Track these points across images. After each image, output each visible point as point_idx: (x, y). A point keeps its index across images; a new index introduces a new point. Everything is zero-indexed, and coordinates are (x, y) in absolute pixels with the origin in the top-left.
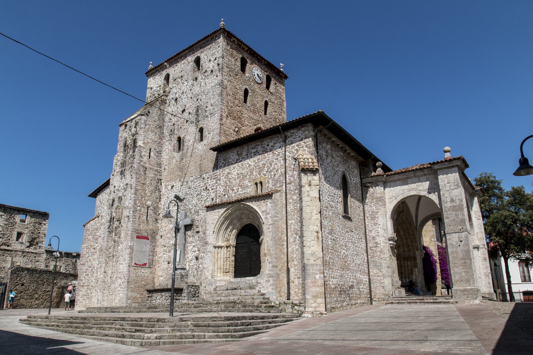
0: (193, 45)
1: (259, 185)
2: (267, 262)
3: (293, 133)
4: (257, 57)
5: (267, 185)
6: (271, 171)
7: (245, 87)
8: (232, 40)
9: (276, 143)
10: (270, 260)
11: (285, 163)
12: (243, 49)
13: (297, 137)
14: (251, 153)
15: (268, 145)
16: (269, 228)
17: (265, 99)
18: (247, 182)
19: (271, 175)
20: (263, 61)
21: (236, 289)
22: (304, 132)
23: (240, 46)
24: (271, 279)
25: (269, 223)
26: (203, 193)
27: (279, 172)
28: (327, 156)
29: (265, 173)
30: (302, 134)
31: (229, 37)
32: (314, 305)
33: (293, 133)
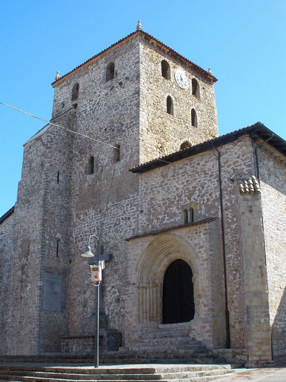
0: (105, 50)
1: (189, 213)
3: (228, 149)
4: (180, 60)
5: (199, 212)
6: (203, 196)
7: (167, 95)
8: (150, 42)
9: (208, 162)
11: (220, 184)
12: (164, 51)
13: (233, 153)
14: (179, 174)
15: (198, 164)
16: (203, 264)
17: (192, 108)
18: (174, 208)
19: (204, 200)
20: (187, 63)
21: (166, 337)
22: (241, 147)
23: (160, 48)
24: (207, 325)
25: (203, 258)
26: (121, 224)
27: (214, 196)
28: (269, 175)
29: (196, 197)
30: (239, 150)
31: (147, 39)
32: (259, 353)
33: (228, 149)
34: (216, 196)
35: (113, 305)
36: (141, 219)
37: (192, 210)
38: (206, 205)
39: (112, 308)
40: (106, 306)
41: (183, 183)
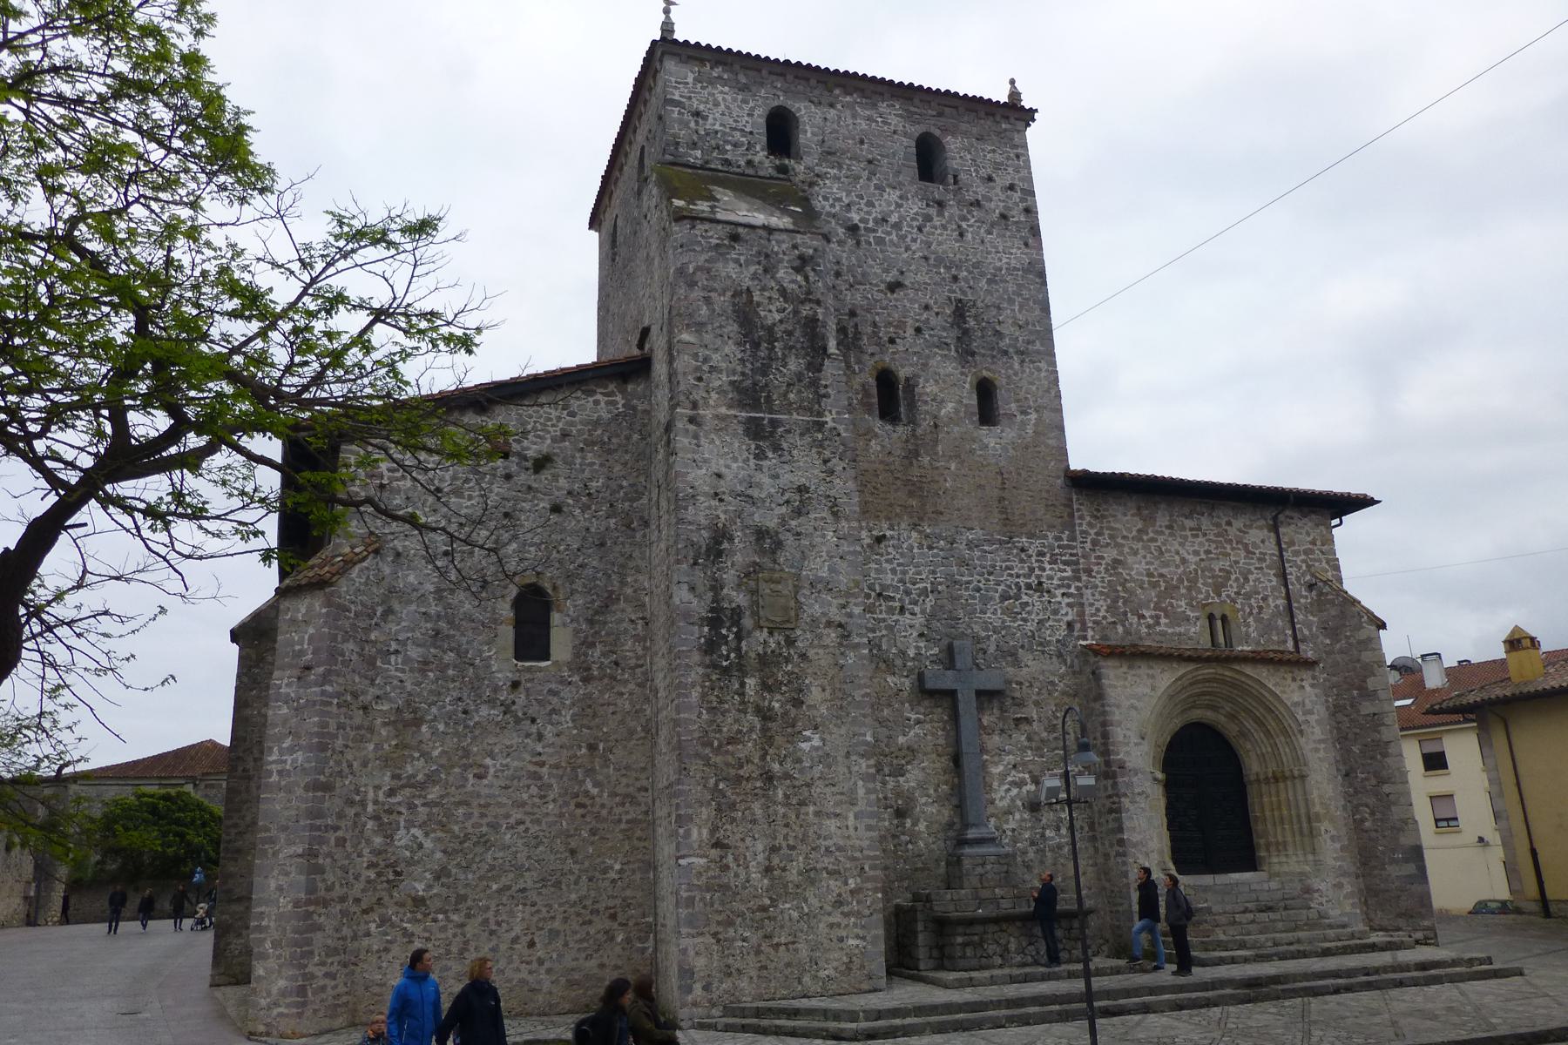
2: (1326, 837)
6: (1248, 596)
9: (1250, 527)
10: (1334, 832)
11: (1286, 586)
15: (1229, 524)
18: (1183, 603)
19: (1251, 607)
24: (1344, 881)
34: (1277, 606)
35: (1017, 816)
36: (1091, 605)
37: (1224, 618)
38: (1258, 620)
39: (1012, 825)
40: (993, 820)
41: (1196, 553)
